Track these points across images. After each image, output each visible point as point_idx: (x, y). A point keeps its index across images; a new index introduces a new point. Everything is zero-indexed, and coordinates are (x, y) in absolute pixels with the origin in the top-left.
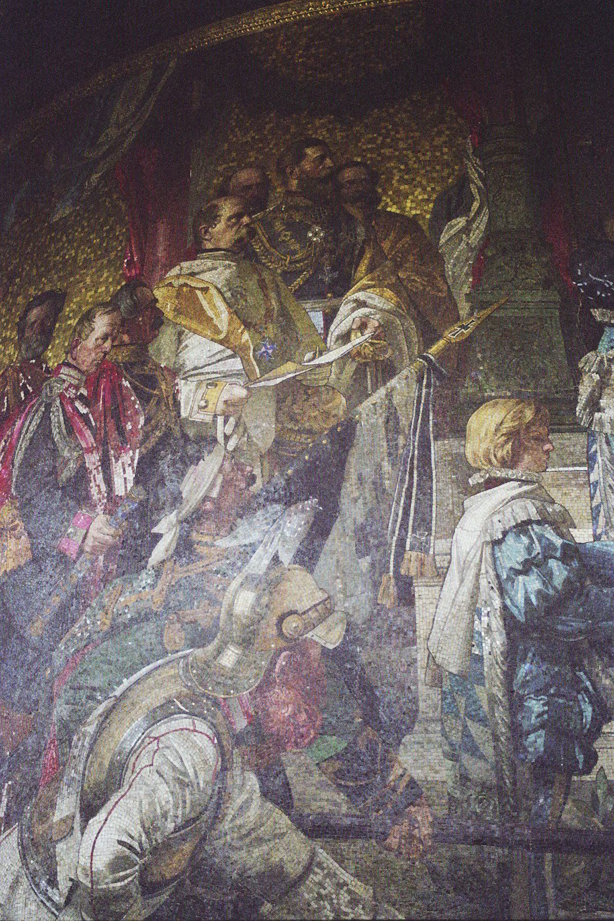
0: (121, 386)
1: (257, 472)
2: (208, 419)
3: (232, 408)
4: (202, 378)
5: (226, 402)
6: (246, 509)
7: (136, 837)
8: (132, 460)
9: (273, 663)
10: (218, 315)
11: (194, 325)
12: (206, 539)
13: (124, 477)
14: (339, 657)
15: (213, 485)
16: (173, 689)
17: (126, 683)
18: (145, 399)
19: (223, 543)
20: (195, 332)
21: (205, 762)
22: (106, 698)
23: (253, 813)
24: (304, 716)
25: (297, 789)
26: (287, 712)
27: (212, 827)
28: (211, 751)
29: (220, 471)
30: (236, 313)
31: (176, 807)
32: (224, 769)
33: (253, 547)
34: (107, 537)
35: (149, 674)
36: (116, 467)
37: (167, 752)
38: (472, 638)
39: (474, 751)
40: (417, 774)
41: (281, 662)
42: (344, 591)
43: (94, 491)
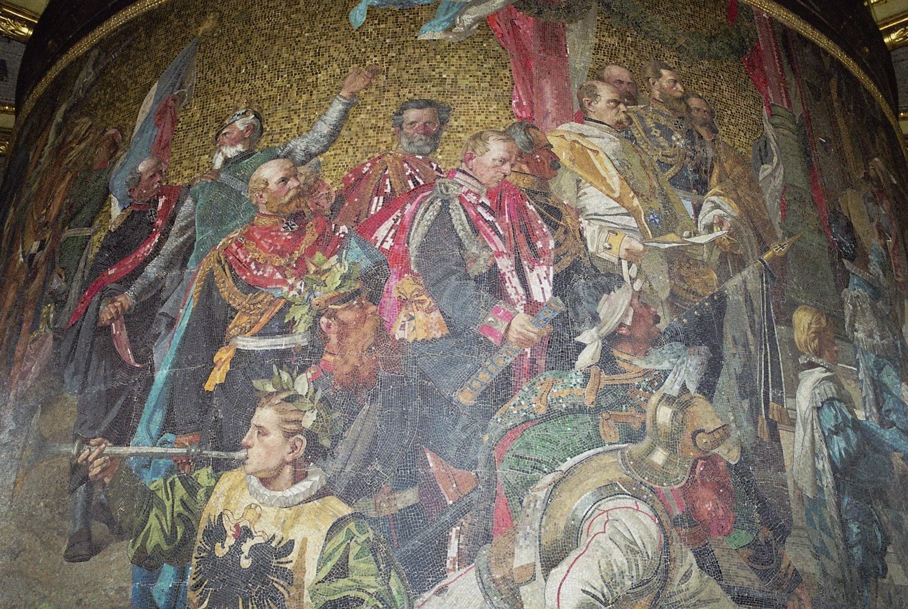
0: (525, 208)
1: (660, 314)
2: (615, 260)
3: (632, 257)
4: (603, 224)
5: (627, 250)
6: (655, 342)
7: (599, 588)
8: (548, 275)
9: (694, 467)
10: (611, 178)
11: (590, 179)
12: (625, 357)
13: (541, 285)
14: (740, 470)
15: (626, 315)
16: (615, 474)
17: (570, 462)
18: (554, 227)
19: (641, 364)
20: (591, 184)
21: (650, 536)
22: (553, 470)
23: (694, 582)
24: (721, 512)
25: (724, 565)
26: (709, 506)
27: (662, 588)
28: (654, 529)
29: (631, 305)
30: (625, 179)
31: (630, 569)
32: (667, 544)
33: (666, 374)
34: (533, 335)
35: (589, 458)
36: (532, 278)
37: (616, 524)
38: (816, 472)
39: (828, 555)
40: (798, 566)
41: (700, 468)
42: (735, 421)
43: (510, 291)
